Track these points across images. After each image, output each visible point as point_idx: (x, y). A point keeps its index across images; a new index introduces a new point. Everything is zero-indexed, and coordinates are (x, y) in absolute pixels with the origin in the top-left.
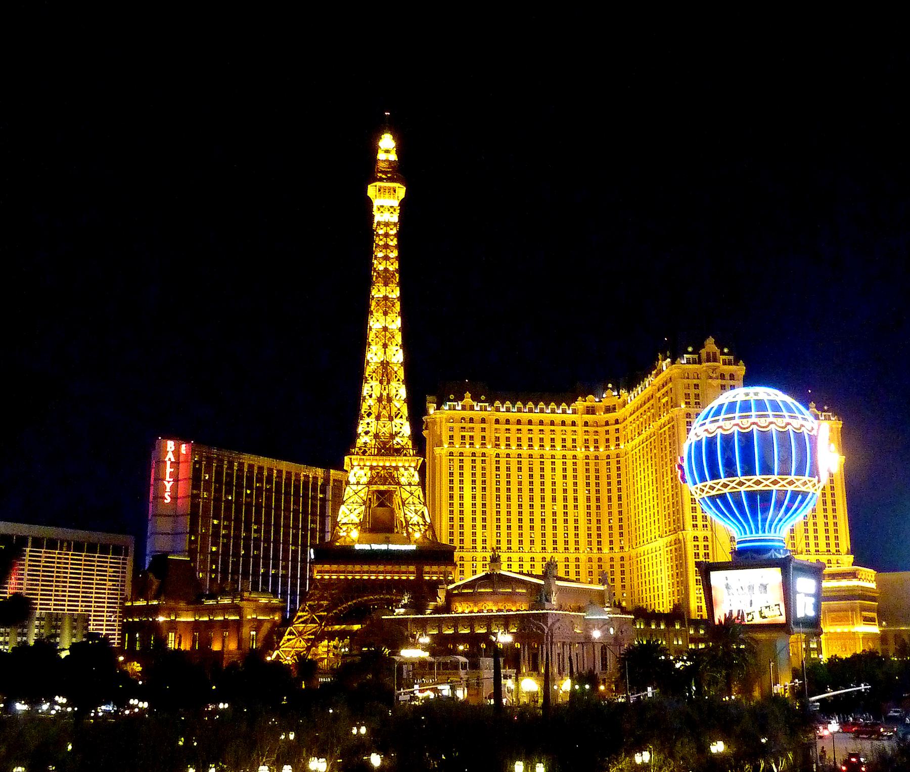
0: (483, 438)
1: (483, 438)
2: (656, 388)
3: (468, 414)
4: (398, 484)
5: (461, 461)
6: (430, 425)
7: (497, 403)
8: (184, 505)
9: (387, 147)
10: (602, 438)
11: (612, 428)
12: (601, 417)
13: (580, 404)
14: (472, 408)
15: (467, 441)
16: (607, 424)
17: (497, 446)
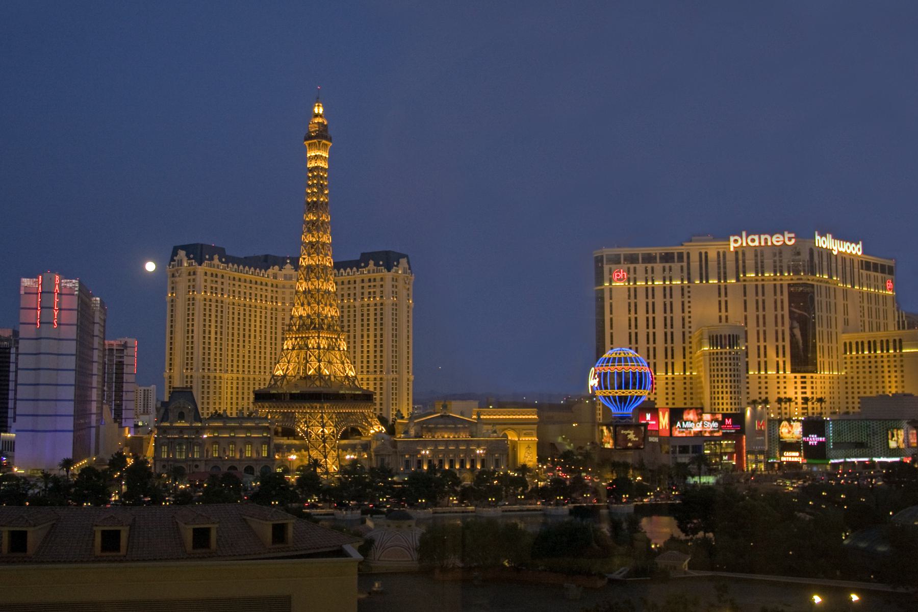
3: (214, 270)
7: (230, 265)
15: (214, 291)
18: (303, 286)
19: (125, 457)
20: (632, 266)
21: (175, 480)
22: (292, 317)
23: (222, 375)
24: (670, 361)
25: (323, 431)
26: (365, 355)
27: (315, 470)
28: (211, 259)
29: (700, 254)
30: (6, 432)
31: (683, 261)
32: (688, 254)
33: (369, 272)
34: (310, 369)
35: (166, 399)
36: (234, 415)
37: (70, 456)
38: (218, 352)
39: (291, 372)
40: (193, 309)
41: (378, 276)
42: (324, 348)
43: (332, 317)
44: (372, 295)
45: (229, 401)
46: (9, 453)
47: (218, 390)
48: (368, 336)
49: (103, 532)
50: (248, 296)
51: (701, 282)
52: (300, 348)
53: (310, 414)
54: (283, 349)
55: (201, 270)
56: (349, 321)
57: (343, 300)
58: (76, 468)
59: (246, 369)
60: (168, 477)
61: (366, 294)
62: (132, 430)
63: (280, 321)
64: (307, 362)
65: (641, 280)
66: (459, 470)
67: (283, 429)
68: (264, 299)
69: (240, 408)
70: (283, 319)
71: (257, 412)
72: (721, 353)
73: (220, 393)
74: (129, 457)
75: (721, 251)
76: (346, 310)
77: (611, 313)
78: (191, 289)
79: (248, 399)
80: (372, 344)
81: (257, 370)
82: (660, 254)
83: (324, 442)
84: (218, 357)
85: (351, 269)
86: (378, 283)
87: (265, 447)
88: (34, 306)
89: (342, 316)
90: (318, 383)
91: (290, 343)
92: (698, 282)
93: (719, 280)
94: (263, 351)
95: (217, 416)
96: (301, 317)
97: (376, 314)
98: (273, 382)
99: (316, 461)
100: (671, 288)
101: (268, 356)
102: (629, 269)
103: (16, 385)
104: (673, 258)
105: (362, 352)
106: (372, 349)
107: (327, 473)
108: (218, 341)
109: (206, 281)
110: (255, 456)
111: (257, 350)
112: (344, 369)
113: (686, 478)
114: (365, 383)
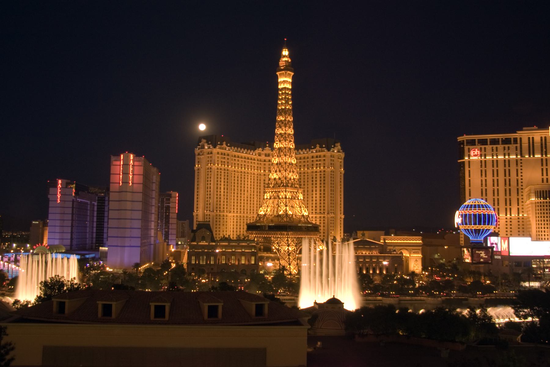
0: (228, 162)
1: (228, 162)
2: (310, 156)
3: (223, 151)
4: (298, 199)
5: (221, 172)
6: (205, 154)
8: (140, 188)
9: (285, 52)
10: (262, 166)
11: (267, 163)
12: (263, 157)
13: (257, 151)
14: (225, 149)
16: (265, 161)
17: (232, 166)
18: (275, 160)
19: (171, 262)
20: (483, 147)
21: (199, 277)
22: (269, 179)
23: (228, 214)
24: (508, 207)
25: (288, 249)
26: (314, 202)
27: (283, 272)
28: (221, 144)
29: (529, 138)
30: (102, 246)
31: (517, 143)
32: (521, 139)
33: (316, 152)
34: (280, 211)
35: (195, 228)
36: (235, 238)
37: (138, 260)
38: (225, 200)
39: (269, 212)
40: (211, 175)
41: (322, 154)
42: (289, 198)
43: (294, 179)
44: (318, 166)
45: (232, 230)
46: (104, 259)
47: (225, 223)
48: (316, 191)
49: (156, 306)
50: (243, 166)
51: (530, 156)
52: (275, 198)
53: (280, 238)
54: (264, 199)
55: (215, 151)
56: (304, 182)
57: (300, 169)
58: (142, 268)
59: (242, 211)
60: (195, 276)
61: (315, 165)
62: (175, 246)
63: (262, 182)
64: (279, 206)
65: (489, 155)
66: (372, 274)
67: (264, 247)
68: (253, 168)
69: (238, 234)
70: (264, 180)
71: (248, 236)
72: (544, 202)
73: (227, 225)
74: (173, 263)
75: (543, 136)
76: (302, 175)
77: (470, 177)
78: (209, 163)
79: (243, 228)
80: (318, 196)
81: (249, 211)
82: (502, 139)
83: (289, 255)
84: (225, 203)
85: (306, 150)
86: (322, 159)
87: (253, 258)
88: (118, 173)
89: (300, 179)
90: (285, 219)
91: (268, 195)
92: (527, 156)
93: (542, 155)
94: (252, 199)
95: (225, 239)
96: (275, 179)
97: (321, 177)
98: (258, 219)
99: (284, 267)
100: (509, 161)
101: (255, 203)
102: (481, 148)
103: (108, 219)
104: (511, 141)
105: (312, 200)
106: (318, 199)
107: (290, 274)
108: (226, 194)
109: (218, 157)
110: (247, 263)
111: (249, 199)
112: (301, 211)
113: (519, 283)
114: (314, 219)
